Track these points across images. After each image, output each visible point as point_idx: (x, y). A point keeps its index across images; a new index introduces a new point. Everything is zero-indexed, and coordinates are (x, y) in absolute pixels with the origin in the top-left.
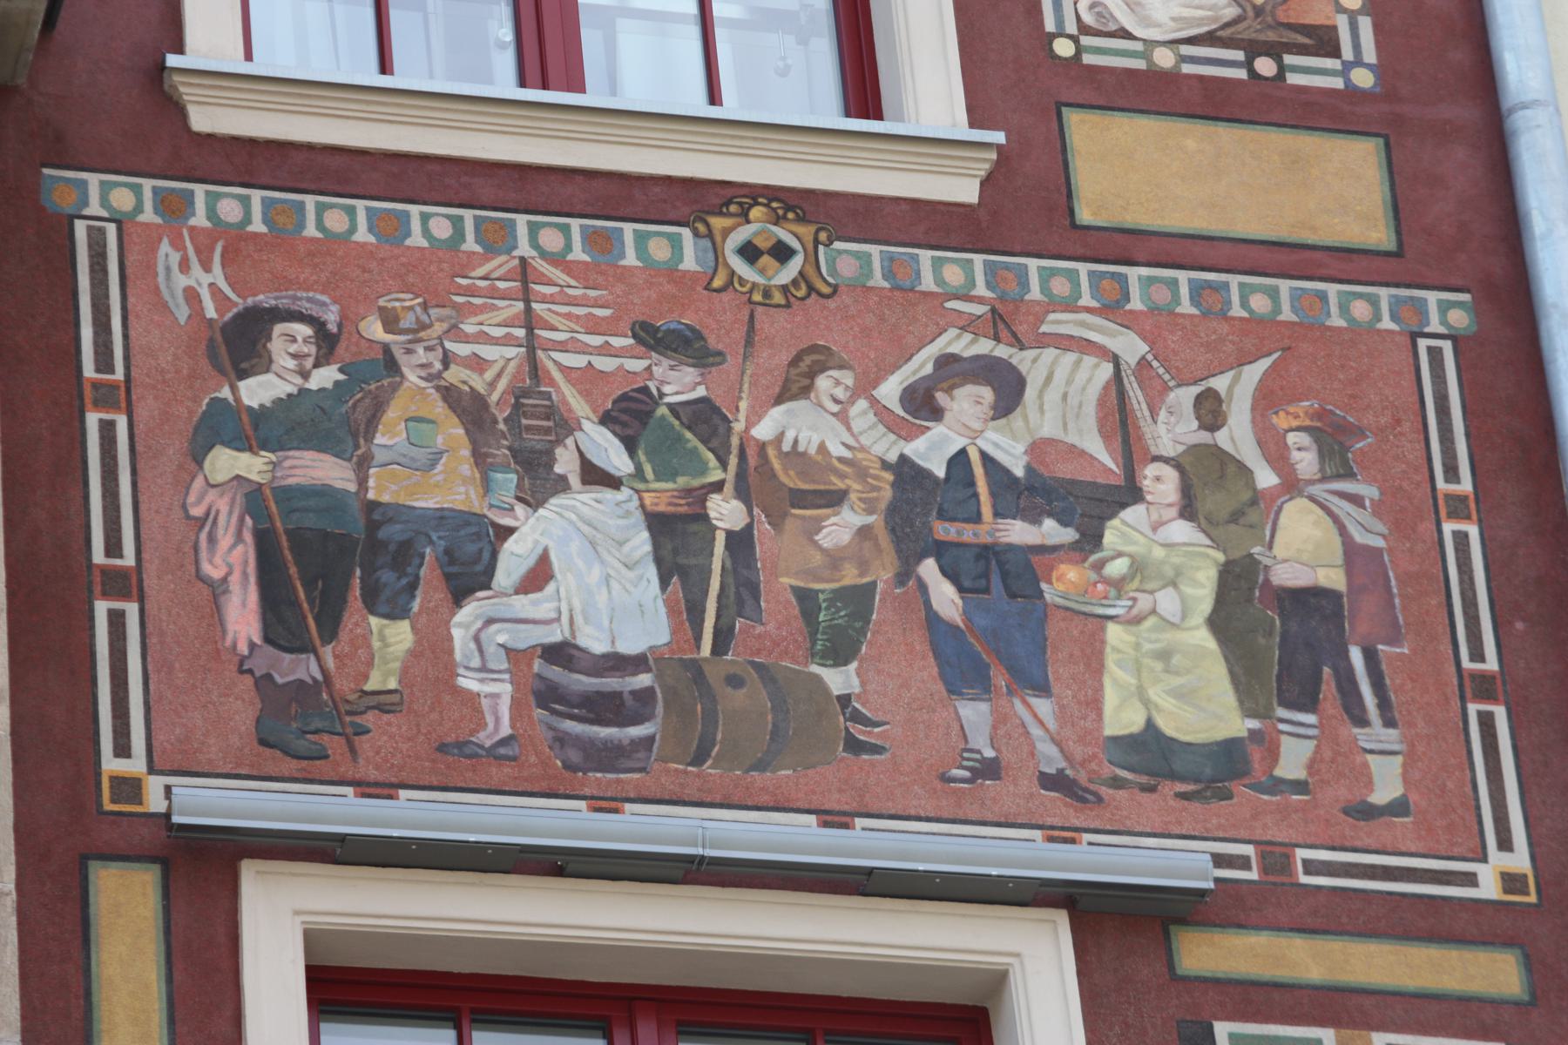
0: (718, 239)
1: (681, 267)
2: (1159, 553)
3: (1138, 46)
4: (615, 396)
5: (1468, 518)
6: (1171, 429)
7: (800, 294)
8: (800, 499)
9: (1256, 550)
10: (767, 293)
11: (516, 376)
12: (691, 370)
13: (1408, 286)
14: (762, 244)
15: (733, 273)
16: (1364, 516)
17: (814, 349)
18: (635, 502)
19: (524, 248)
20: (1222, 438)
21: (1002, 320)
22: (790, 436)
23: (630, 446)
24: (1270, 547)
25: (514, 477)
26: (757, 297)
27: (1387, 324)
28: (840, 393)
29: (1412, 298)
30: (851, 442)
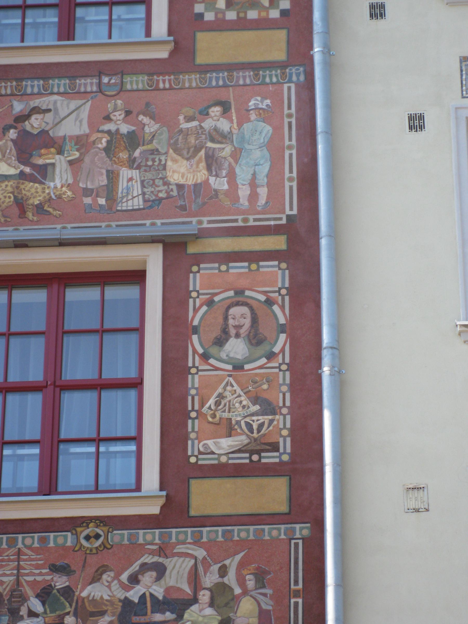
0: (79, 534)
1: (67, 545)
2: (201, 619)
3: (216, 456)
4: (41, 588)
5: (299, 597)
6: (210, 579)
7: (101, 549)
8: (93, 614)
9: (231, 615)
10: (91, 550)
11: (13, 586)
12: (65, 577)
13: (291, 523)
14: (92, 535)
15: (81, 545)
16: (267, 600)
17: (103, 566)
18: (43, 621)
19: (20, 545)
20: (226, 580)
21: (163, 551)
22: (92, 594)
23: (44, 603)
24: (236, 613)
25: (7, 618)
26: (88, 552)
27: (283, 537)
28: (109, 579)
29: (291, 527)
30: (111, 594)
